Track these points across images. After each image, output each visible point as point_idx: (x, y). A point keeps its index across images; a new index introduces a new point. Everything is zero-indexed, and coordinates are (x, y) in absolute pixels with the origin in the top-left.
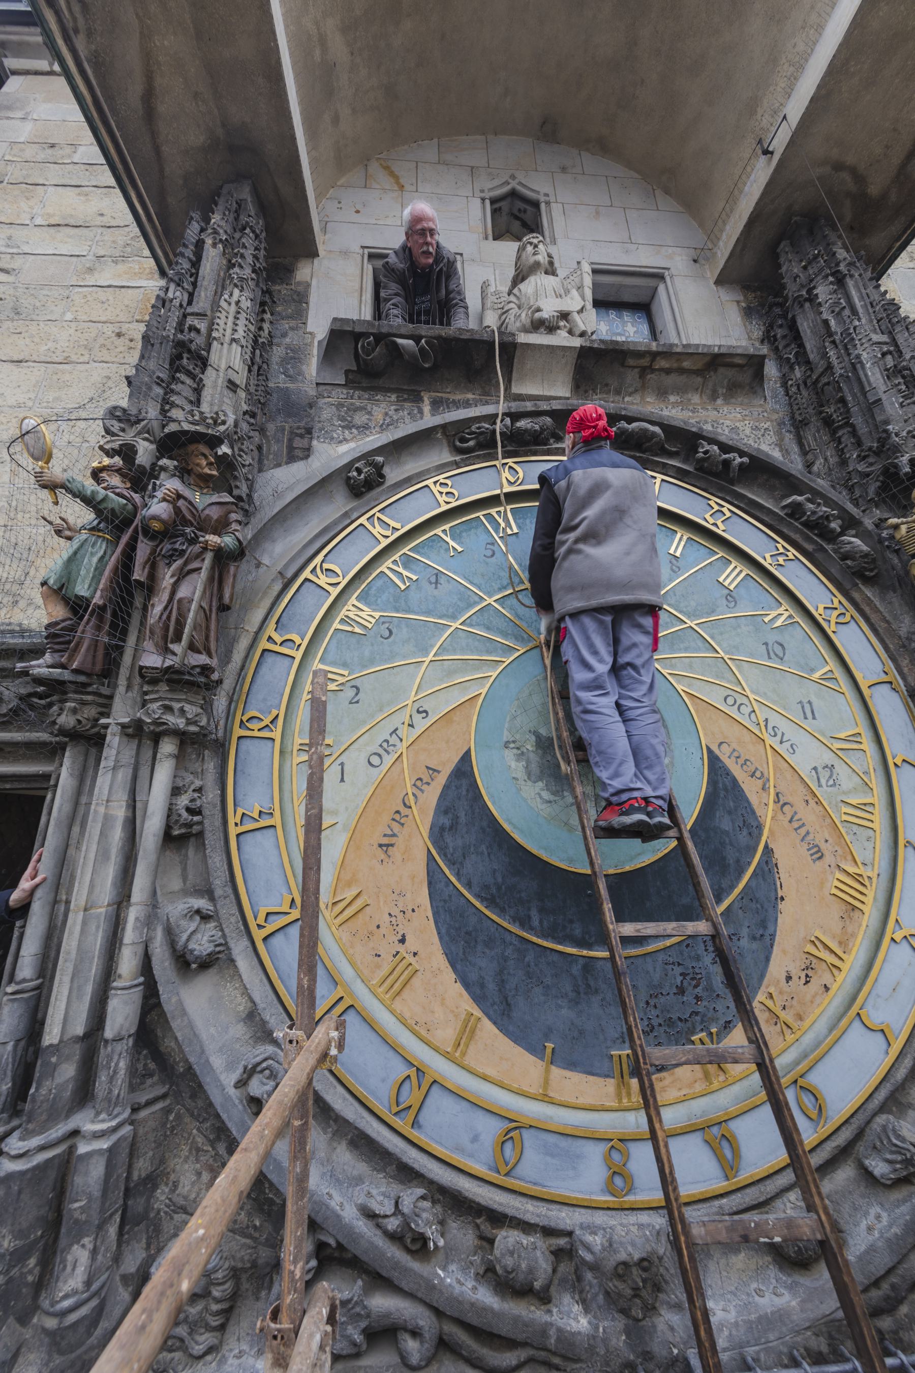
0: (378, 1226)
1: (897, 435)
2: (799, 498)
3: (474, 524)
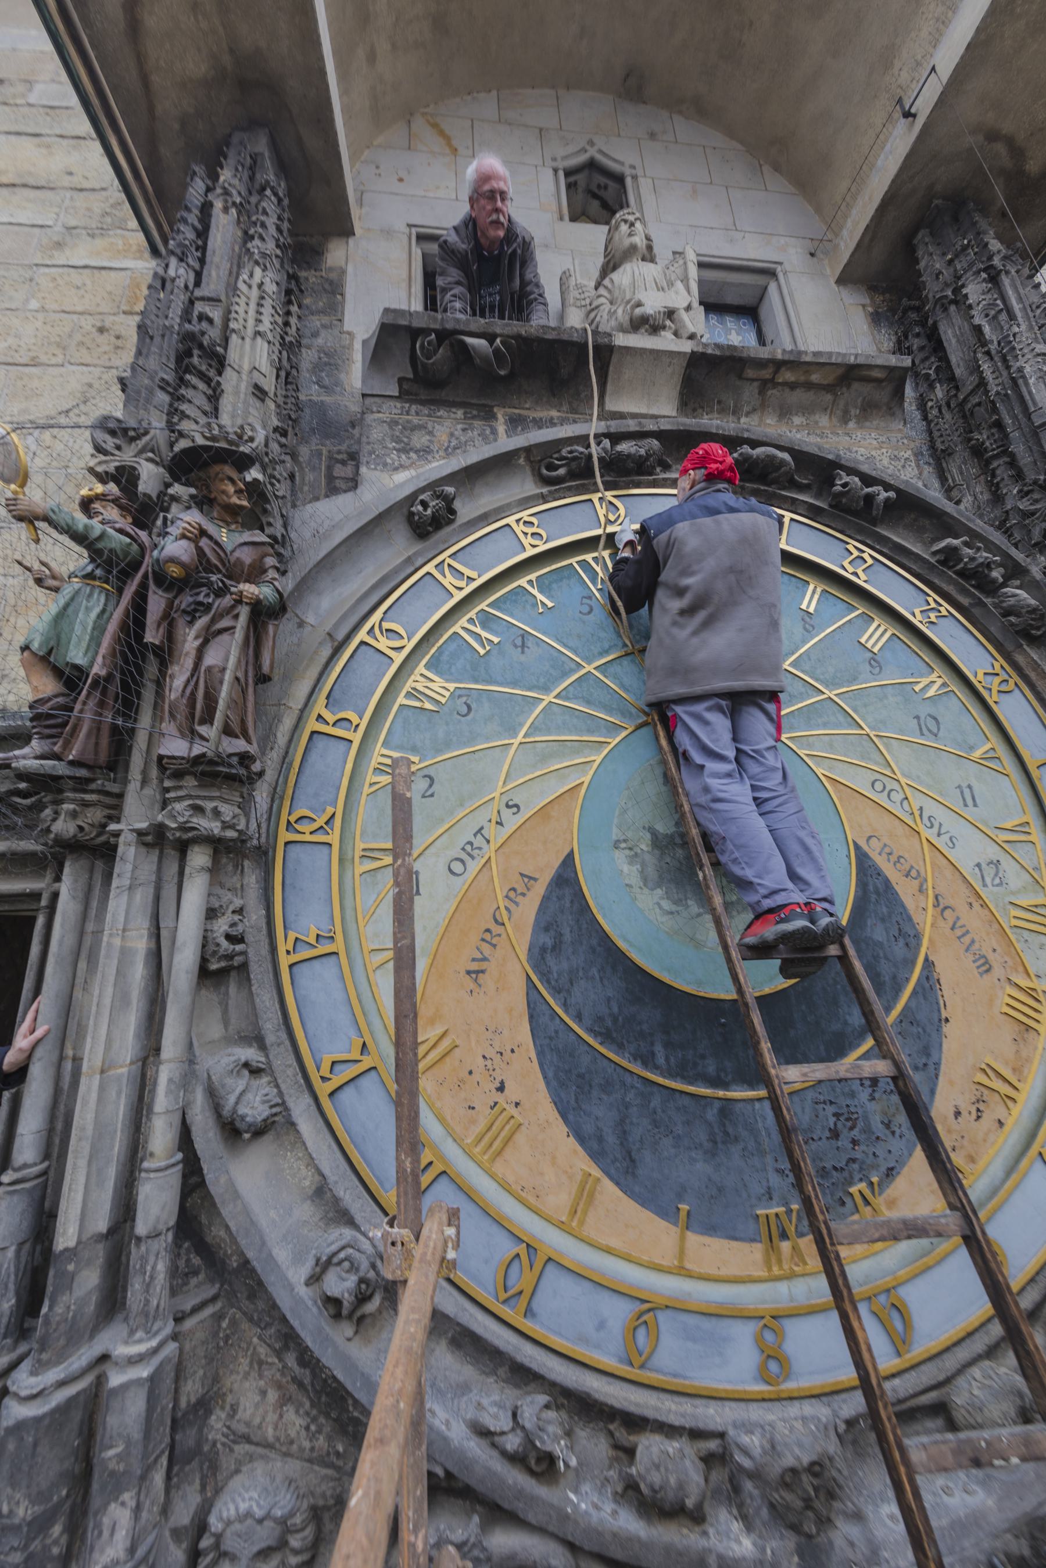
0: (494, 1445)
3: (566, 573)
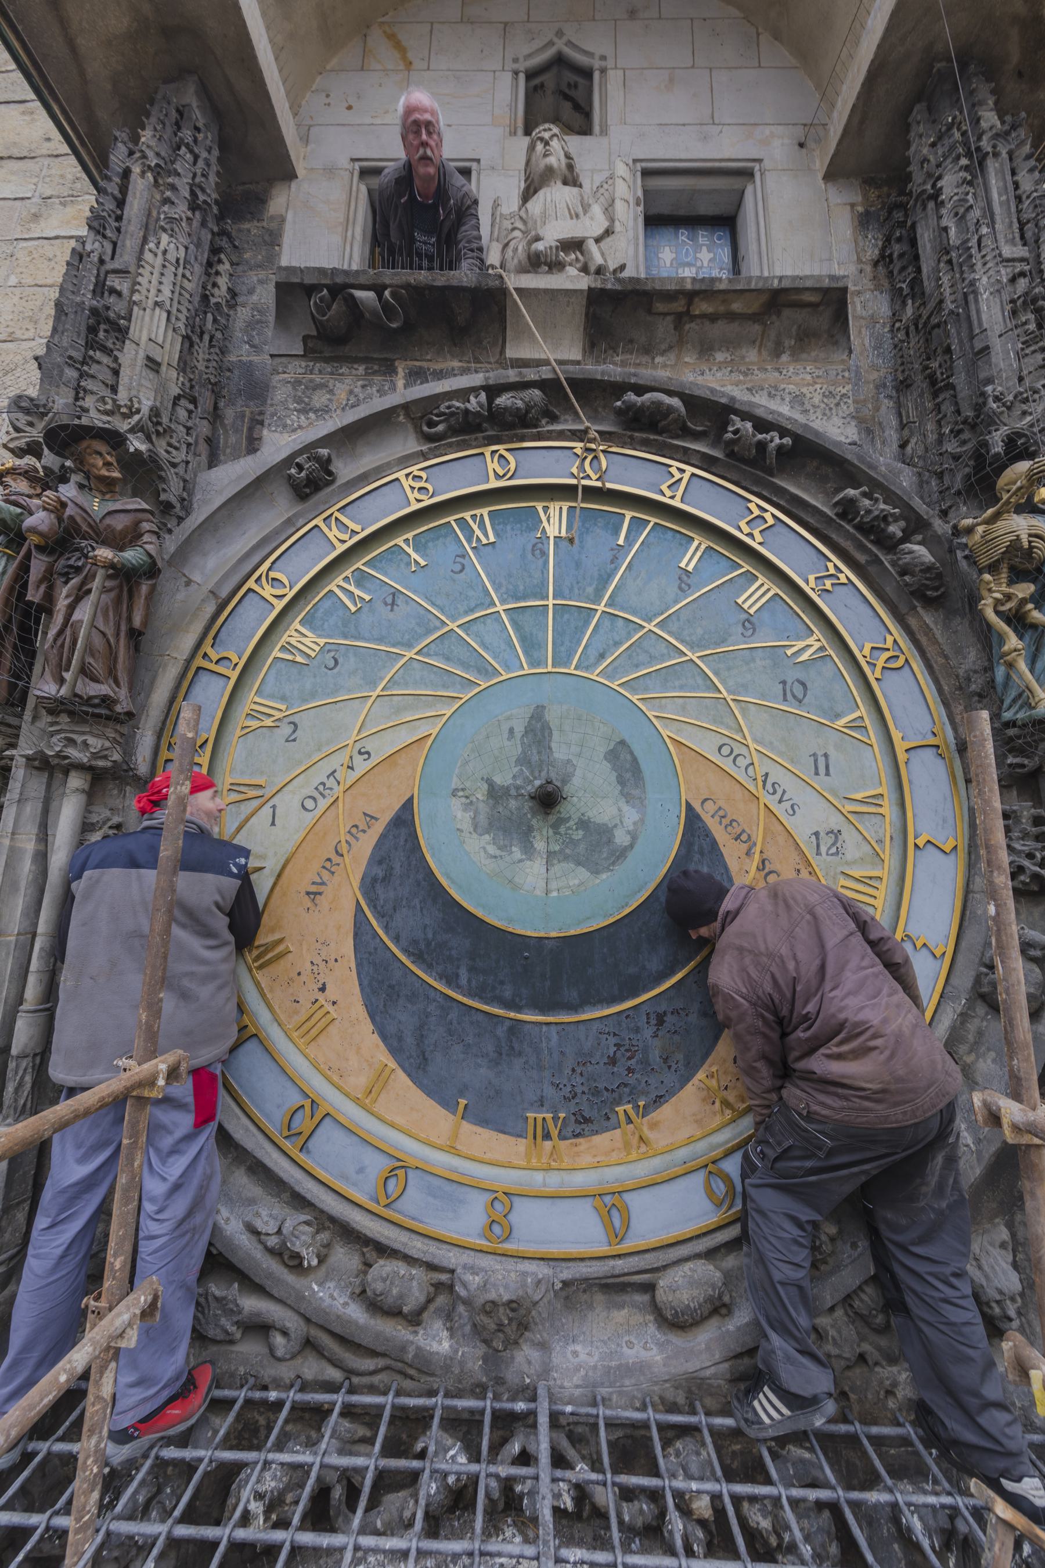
0: (260, 1242)
1: (997, 399)
2: (851, 492)
3: (443, 531)
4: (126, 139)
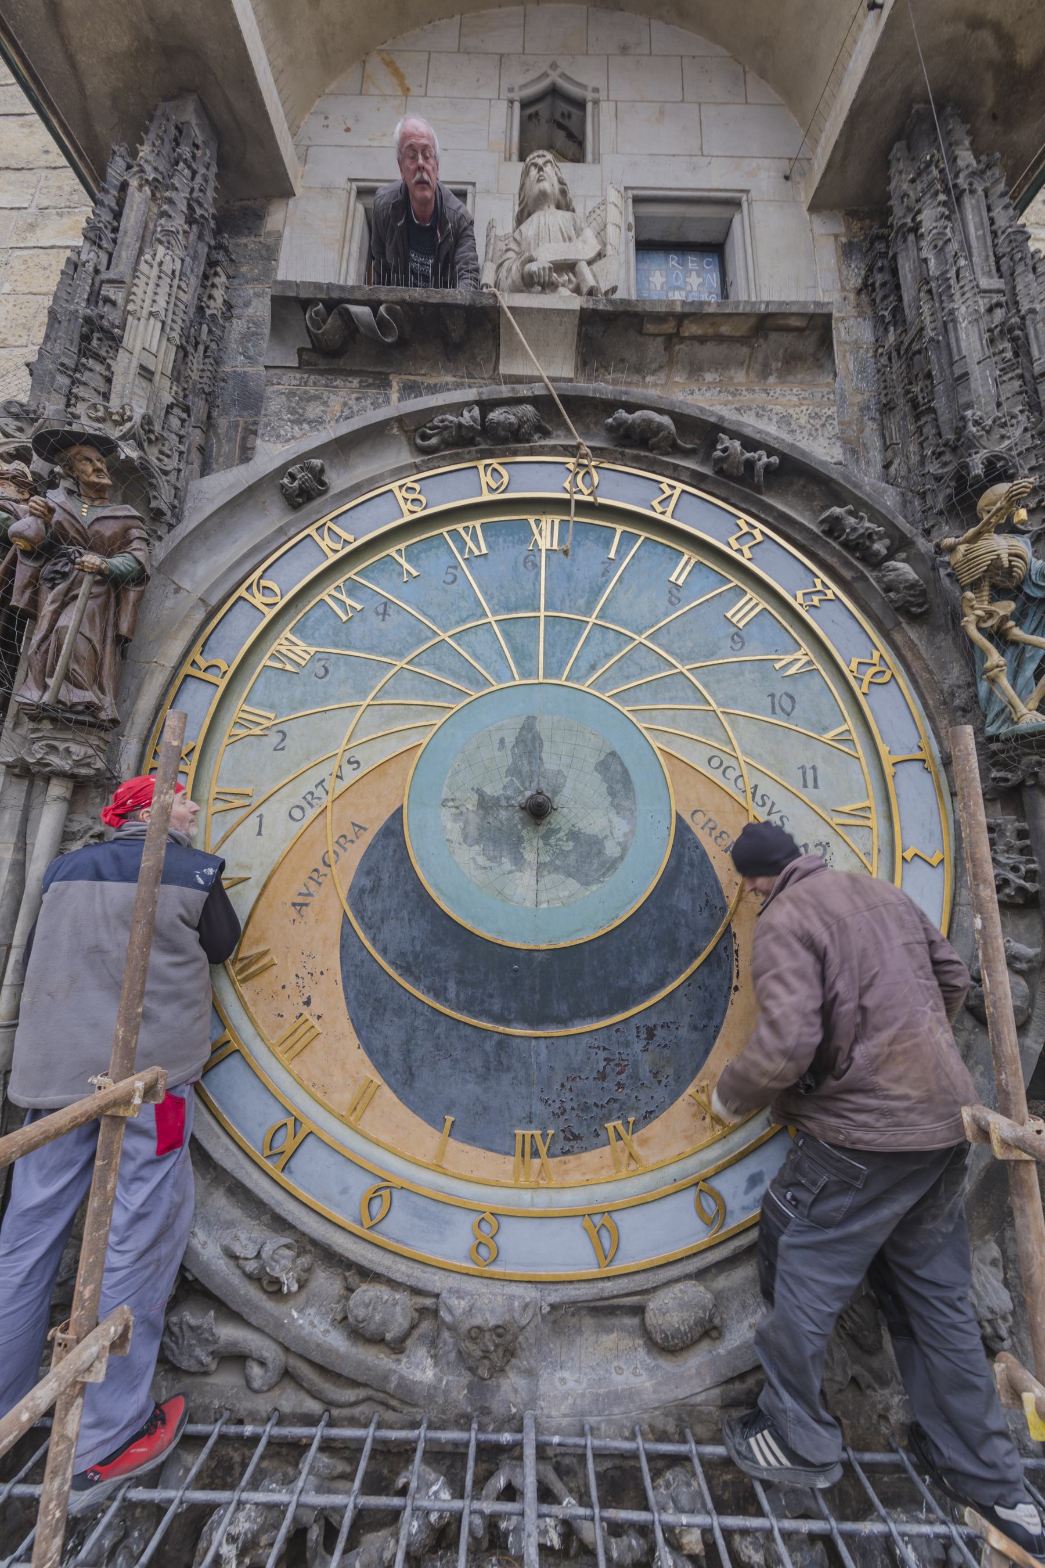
0: (238, 1266)
1: (976, 423)
2: (837, 510)
3: (436, 542)
4: (124, 153)
